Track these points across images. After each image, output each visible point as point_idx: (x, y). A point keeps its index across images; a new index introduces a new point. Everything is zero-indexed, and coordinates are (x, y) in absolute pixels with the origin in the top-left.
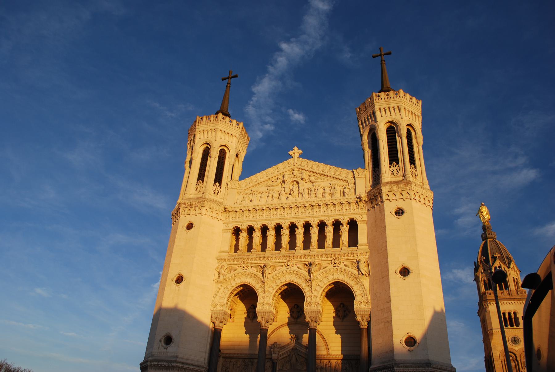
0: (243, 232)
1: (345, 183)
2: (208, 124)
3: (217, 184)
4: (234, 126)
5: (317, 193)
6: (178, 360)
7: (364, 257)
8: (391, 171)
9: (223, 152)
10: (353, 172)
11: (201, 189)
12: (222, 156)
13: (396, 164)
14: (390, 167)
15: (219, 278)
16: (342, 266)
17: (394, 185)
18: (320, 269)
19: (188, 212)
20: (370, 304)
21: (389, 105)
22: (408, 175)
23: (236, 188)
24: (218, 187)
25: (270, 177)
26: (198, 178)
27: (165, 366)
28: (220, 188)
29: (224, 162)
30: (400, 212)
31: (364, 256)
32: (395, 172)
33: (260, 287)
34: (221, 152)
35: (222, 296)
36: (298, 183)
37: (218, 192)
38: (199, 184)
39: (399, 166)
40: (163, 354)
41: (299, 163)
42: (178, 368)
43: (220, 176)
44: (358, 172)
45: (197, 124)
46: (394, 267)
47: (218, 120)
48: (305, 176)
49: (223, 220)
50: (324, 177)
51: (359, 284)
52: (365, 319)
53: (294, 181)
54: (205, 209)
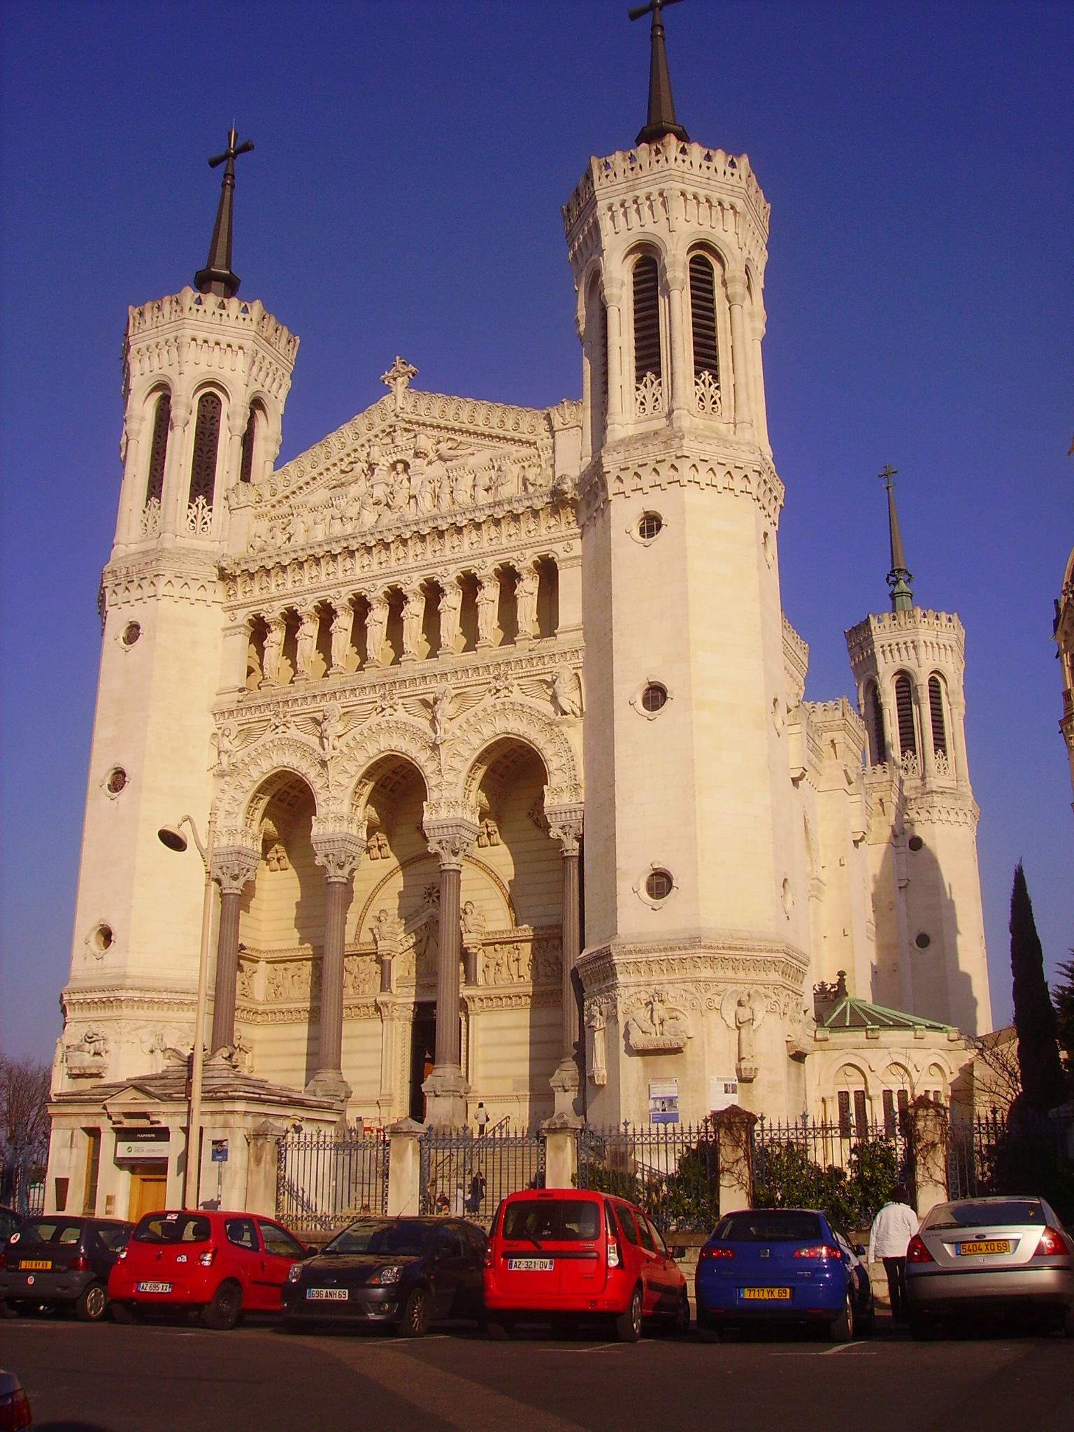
0: (273, 628)
1: (532, 451)
2: (157, 327)
3: (201, 500)
4: (233, 317)
6: (128, 982)
7: (571, 662)
8: (639, 401)
9: (213, 402)
10: (548, 418)
12: (209, 416)
13: (653, 379)
14: (638, 389)
16: (517, 695)
17: (635, 446)
18: (463, 709)
19: (125, 595)
20: (582, 792)
21: (636, 193)
22: (677, 409)
24: (204, 507)
25: (334, 459)
26: (149, 490)
28: (210, 510)
29: (218, 430)
30: (651, 525)
31: (571, 659)
32: (649, 404)
33: (319, 775)
34: (207, 401)
36: (407, 466)
37: (205, 523)
39: (660, 384)
41: (409, 408)
43: (208, 475)
44: (563, 415)
46: (628, 690)
47: (182, 310)
48: (425, 443)
50: (479, 441)
51: (557, 740)
52: (572, 832)
54: (164, 580)
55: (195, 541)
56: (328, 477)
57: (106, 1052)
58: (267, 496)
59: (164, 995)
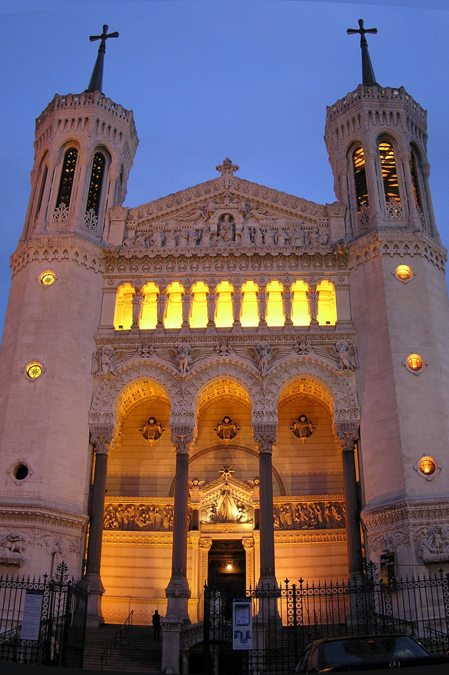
1: (313, 225)
5: (265, 236)
6: (42, 503)
11: (65, 217)
15: (100, 369)
23: (124, 219)
24: (93, 216)
25: (183, 205)
27: (20, 513)
28: (97, 218)
35: (107, 401)
36: (231, 218)
37: (94, 225)
38: (60, 209)
40: (13, 493)
42: (42, 518)
45: (56, 108)
47: (93, 102)
49: (102, 272)
53: (227, 214)
55: (88, 234)
56: (177, 215)
57: (23, 550)
58: (136, 218)
59: (63, 516)
